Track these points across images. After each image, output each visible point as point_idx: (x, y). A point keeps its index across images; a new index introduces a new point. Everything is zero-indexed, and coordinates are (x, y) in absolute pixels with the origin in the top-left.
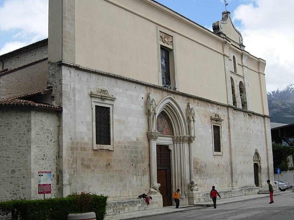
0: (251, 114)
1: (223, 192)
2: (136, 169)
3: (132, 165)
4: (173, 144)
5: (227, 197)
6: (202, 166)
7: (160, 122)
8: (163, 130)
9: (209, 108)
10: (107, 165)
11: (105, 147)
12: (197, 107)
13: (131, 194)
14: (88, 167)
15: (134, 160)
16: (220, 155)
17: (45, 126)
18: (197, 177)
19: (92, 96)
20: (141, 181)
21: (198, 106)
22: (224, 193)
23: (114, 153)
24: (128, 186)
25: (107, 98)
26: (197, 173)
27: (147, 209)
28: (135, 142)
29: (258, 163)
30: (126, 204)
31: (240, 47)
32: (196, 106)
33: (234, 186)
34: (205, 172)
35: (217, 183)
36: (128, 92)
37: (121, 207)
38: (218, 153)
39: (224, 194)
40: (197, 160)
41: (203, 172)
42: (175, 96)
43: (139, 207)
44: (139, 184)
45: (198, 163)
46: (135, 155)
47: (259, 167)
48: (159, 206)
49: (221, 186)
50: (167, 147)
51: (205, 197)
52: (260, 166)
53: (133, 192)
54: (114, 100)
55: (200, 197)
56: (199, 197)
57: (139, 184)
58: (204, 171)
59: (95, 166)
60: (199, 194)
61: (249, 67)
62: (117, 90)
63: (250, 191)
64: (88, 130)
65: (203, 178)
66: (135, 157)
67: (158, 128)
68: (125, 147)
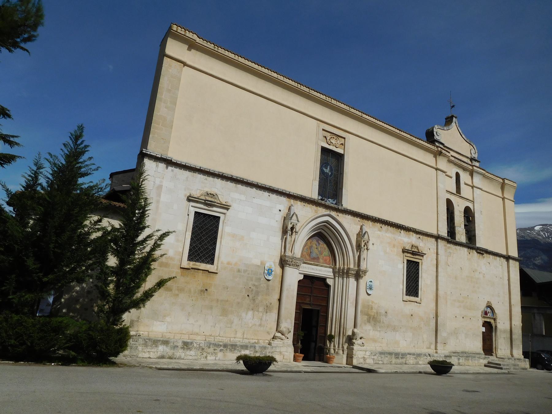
0: (482, 252)
1: (414, 354)
2: (254, 302)
3: (248, 296)
4: (333, 277)
5: (420, 362)
6: (380, 313)
7: (314, 246)
8: (318, 257)
10: (202, 291)
11: (203, 266)
12: (379, 232)
13: (239, 335)
16: (416, 302)
18: (368, 327)
19: (190, 199)
20: (261, 319)
21: (380, 231)
22: (415, 356)
23: (217, 276)
25: (216, 204)
26: (369, 321)
28: (258, 266)
29: (492, 321)
31: (472, 162)
32: (377, 230)
33: (438, 349)
35: (406, 340)
36: (255, 201)
37: (211, 350)
39: (415, 358)
40: (371, 303)
42: (340, 215)
44: (258, 324)
45: (372, 308)
46: (256, 284)
47: (494, 327)
48: (283, 358)
50: (323, 280)
51: (375, 357)
52: (496, 327)
53: (244, 334)
54: (228, 209)
55: (365, 356)
56: (365, 355)
57: (257, 324)
59: (181, 290)
61: (484, 189)
62: (236, 196)
63: (468, 360)
65: (379, 329)
66: (254, 285)
67: (311, 253)
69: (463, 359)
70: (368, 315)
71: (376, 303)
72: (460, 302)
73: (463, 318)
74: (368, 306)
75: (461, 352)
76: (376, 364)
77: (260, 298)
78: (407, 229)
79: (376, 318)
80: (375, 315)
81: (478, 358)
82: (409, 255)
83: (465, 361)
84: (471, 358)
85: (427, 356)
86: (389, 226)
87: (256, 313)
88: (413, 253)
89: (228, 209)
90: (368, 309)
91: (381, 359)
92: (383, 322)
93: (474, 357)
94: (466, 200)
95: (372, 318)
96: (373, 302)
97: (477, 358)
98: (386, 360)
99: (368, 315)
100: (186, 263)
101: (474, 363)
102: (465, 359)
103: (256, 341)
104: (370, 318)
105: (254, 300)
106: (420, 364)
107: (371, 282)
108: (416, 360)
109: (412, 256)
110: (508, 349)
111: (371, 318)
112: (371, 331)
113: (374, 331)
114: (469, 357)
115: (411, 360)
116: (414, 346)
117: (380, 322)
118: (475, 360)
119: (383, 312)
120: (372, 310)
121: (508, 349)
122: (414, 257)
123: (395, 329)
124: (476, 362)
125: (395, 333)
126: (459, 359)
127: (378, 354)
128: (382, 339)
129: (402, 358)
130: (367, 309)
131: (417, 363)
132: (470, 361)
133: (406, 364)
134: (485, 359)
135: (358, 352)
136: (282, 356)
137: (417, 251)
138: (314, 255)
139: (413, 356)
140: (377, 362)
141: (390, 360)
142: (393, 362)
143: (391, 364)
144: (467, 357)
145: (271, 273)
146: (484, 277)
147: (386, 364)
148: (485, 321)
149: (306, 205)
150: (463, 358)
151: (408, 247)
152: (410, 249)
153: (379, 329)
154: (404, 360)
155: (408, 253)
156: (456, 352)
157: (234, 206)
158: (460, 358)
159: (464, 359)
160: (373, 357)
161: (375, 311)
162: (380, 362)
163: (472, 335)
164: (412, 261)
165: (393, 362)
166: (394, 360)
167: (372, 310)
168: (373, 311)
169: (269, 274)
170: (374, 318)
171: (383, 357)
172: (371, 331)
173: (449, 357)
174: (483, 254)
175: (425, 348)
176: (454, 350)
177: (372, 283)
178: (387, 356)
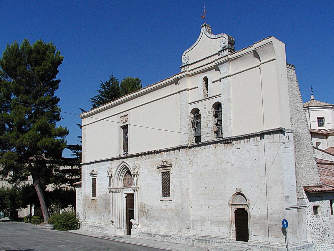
7: (129, 178)
9: (158, 157)
12: (145, 161)
14: (90, 208)
24: (102, 219)
26: (144, 215)
28: (105, 194)
29: (246, 207)
30: (95, 227)
34: (151, 214)
38: (166, 198)
46: (106, 202)
49: (169, 230)
51: (140, 235)
58: (150, 214)
62: (99, 167)
65: (149, 220)
66: (105, 203)
72: (204, 195)
73: (208, 207)
78: (160, 152)
82: (162, 169)
89: (97, 174)
98: (146, 237)
103: (107, 225)
104: (144, 213)
122: (165, 169)
123: (157, 219)
137: (167, 164)
138: (129, 183)
146: (232, 165)
148: (237, 208)
151: (161, 164)
152: (162, 165)
155: (161, 168)
157: (99, 172)
160: (139, 235)
164: (165, 172)
174: (231, 143)
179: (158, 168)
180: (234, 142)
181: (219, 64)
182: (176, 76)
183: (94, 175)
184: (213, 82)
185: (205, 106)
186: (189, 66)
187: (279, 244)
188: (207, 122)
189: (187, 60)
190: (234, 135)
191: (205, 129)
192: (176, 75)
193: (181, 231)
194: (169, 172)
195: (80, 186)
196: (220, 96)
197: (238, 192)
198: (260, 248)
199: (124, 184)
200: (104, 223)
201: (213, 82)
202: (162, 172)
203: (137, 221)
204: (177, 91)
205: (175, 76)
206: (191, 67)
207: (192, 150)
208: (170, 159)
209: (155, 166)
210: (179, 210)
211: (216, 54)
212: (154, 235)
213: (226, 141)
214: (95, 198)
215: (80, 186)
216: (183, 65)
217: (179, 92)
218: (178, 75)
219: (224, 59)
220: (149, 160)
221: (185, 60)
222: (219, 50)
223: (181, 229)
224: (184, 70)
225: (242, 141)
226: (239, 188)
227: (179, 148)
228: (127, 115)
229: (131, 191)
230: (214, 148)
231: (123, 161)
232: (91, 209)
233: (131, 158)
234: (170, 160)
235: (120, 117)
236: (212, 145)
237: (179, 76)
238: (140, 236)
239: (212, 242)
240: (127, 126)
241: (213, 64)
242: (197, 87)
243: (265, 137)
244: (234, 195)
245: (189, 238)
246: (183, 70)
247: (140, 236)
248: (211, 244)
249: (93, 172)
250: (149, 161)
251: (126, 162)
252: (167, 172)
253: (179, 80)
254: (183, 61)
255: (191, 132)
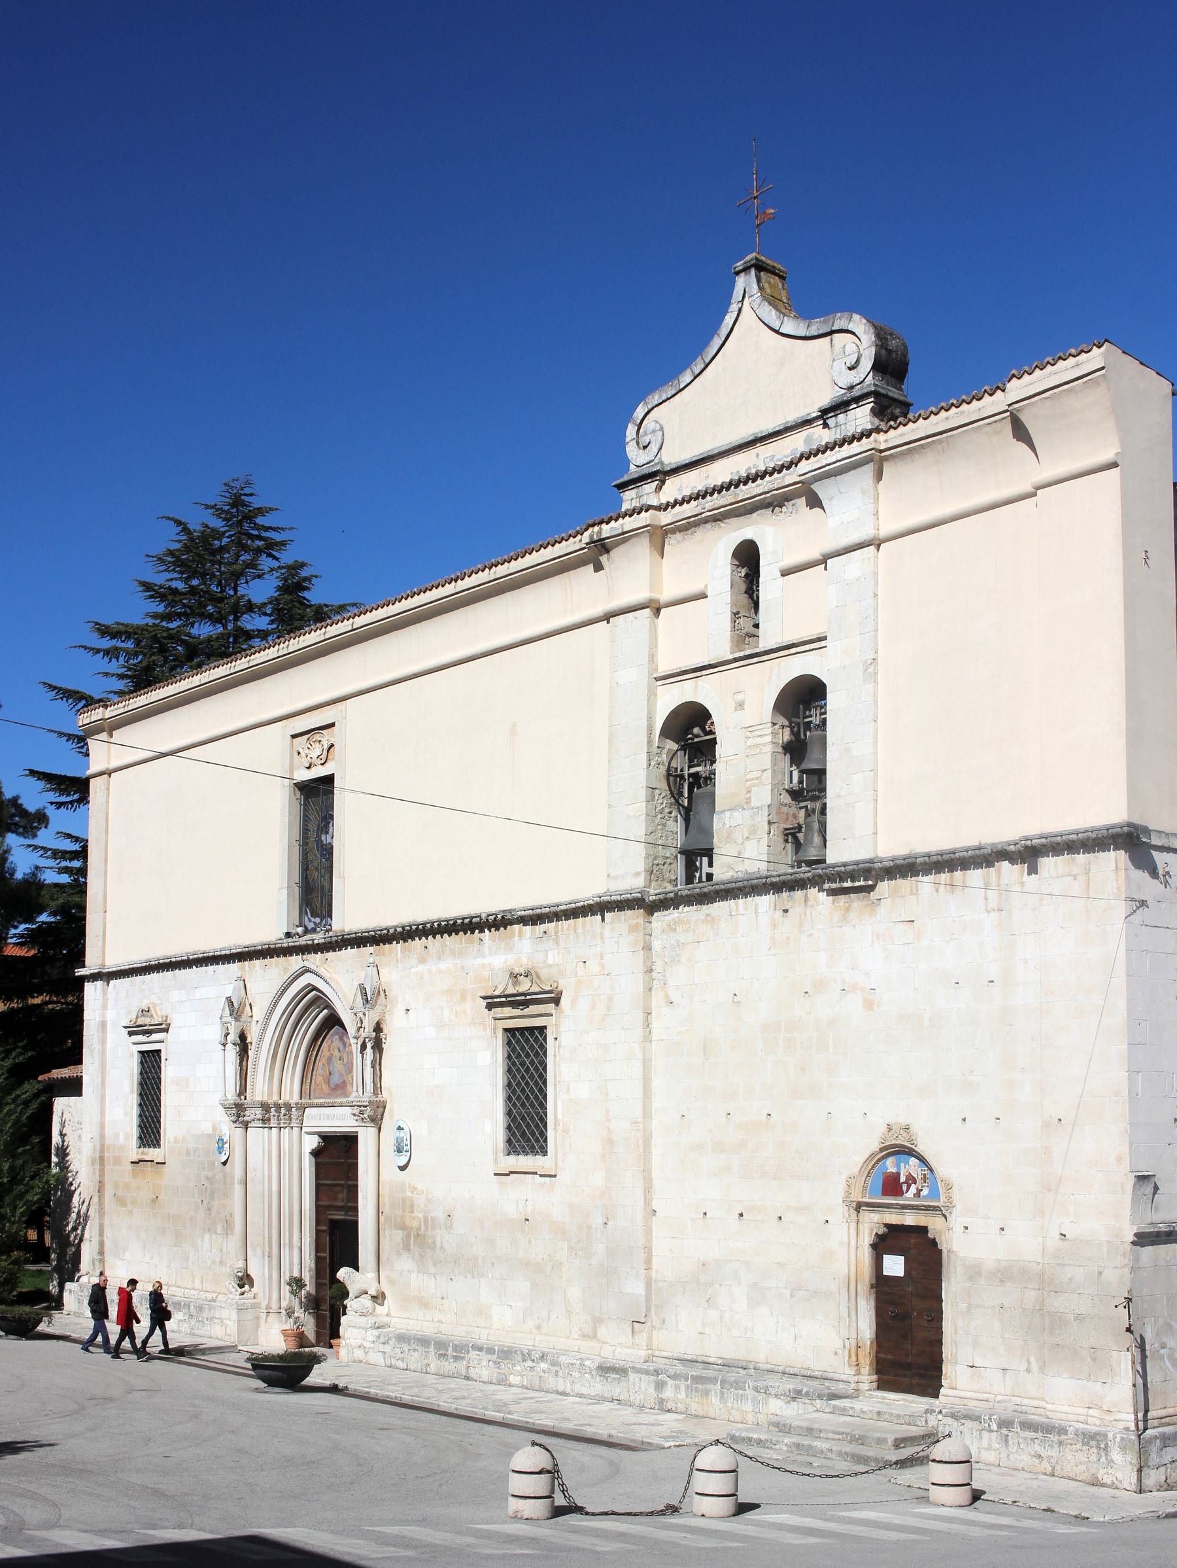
1: (490, 1351)
5: (513, 1379)
6: (432, 1217)
7: (336, 1053)
12: (420, 968)
15: (206, 1189)
17: (75, 1114)
21: (423, 961)
22: (494, 1357)
26: (407, 1247)
27: (197, 1332)
28: (209, 1135)
29: (934, 1223)
39: (495, 1362)
40: (409, 1194)
41: (434, 1243)
43: (180, 1321)
44: (218, 1260)
45: (412, 1206)
46: (210, 1174)
47: (944, 1255)
49: (539, 1327)
51: (387, 1348)
53: (202, 1281)
60: (363, 1328)
62: (175, 996)
63: (707, 1393)
64: (126, 1114)
66: (207, 1178)
67: (330, 1074)
68: (188, 1153)
69: (677, 1387)
70: (403, 1227)
71: (423, 1192)
73: (741, 1215)
74: (404, 1200)
75: (719, 1362)
76: (390, 1367)
77: (216, 1203)
78: (499, 922)
79: (424, 1234)
80: (420, 1229)
81: (756, 1389)
82: (508, 1011)
83: (687, 1397)
84: (718, 1386)
85: (533, 1361)
86: (446, 935)
87: (214, 1236)
88: (521, 1001)
89: (166, 1030)
90: (403, 1212)
91: (401, 1356)
92: (442, 1248)
93: (738, 1385)
94: (782, 653)
95: (414, 1237)
96: (414, 1189)
97: (750, 1392)
98: (415, 1359)
99: (403, 1227)
100: (133, 1151)
101: (733, 1412)
102: (687, 1387)
103: (214, 1295)
104: (408, 1235)
105: (209, 1210)
106: (510, 1385)
107: (400, 1128)
108: (498, 1371)
109: (517, 1012)
110: (1028, 1371)
111: (412, 1238)
112: (414, 1275)
113: (420, 1275)
114: (712, 1380)
115: (483, 1369)
116: (539, 1327)
117: (433, 1247)
118: (742, 1398)
119: (439, 1214)
120: (413, 1213)
121: (1028, 1371)
122: (527, 1011)
124: (748, 1407)
125: (476, 1280)
126: (660, 1386)
127: (394, 1340)
128: (443, 1298)
129: (456, 1358)
130: (401, 1210)
131: (503, 1381)
132: (715, 1400)
133: (467, 1378)
134: (794, 1399)
135: (349, 1329)
136: (224, 1328)
137: (535, 989)
139: (489, 1357)
140: (393, 1362)
141: (425, 1362)
142: (432, 1369)
143: (426, 1373)
144: (697, 1379)
145: (223, 1147)
146: (869, 1005)
147: (415, 1371)
148: (888, 1226)
149: (268, 961)
150: (683, 1385)
151: (503, 986)
152: (511, 990)
153: (432, 1270)
154: (461, 1366)
155: (501, 1005)
156: (697, 1362)
158: (666, 1383)
159: (683, 1387)
160: (381, 1347)
161: (420, 1215)
162: (400, 1364)
163: (787, 1293)
164: (522, 1030)
165: (432, 1369)
166: (435, 1364)
167: (413, 1213)
168: (416, 1214)
169: (220, 1150)
170: (418, 1235)
171: (406, 1350)
172: (414, 1275)
173: (617, 1374)
174: (871, 889)
175: (576, 1336)
176: (691, 1352)
177: (402, 1134)
178: (417, 1348)
179: (490, 1007)
180: (884, 887)
181: (818, 478)
182: (596, 529)
183: (149, 1032)
184: (785, 573)
185: (740, 697)
186: (663, 482)
187: (1091, 1412)
188: (748, 777)
189: (654, 448)
190: (888, 848)
191: (736, 814)
192: (593, 525)
193: (599, 1334)
194: (545, 1027)
195: (74, 1087)
196: (823, 643)
197: (893, 1142)
198: (995, 1427)
199: (306, 1087)
200: (197, 1284)
201: (785, 573)
202: (506, 1030)
203: (372, 1275)
204: (598, 610)
205: (587, 534)
206: (674, 488)
207: (667, 918)
208: (550, 961)
209: (469, 997)
210: (589, 1227)
211: (807, 422)
212: (456, 1348)
213: (842, 877)
214: (152, 1153)
215: (74, 1087)
216: (633, 471)
217: (608, 617)
218: (604, 526)
219: (847, 450)
220: (443, 965)
221: (645, 447)
222: (825, 401)
223: (598, 1321)
224: (636, 504)
225: (925, 883)
226: (903, 1120)
227: (601, 908)
228: (332, 725)
229: (339, 1120)
230: (779, 913)
231: (307, 964)
232: (131, 1212)
233: (349, 953)
234: (550, 966)
235: (294, 737)
236: (765, 901)
237: (607, 530)
238: (384, 1353)
239: (753, 1392)
240: (329, 780)
241: (790, 477)
242: (703, 596)
243: (1047, 864)
244: (872, 1155)
245: (637, 1370)
246: (629, 499)
247: (384, 1353)
248: (748, 1407)
249: (147, 1021)
250: (440, 971)
251: (322, 971)
252: (531, 1030)
253: (607, 551)
254: (631, 450)
255: (664, 825)
